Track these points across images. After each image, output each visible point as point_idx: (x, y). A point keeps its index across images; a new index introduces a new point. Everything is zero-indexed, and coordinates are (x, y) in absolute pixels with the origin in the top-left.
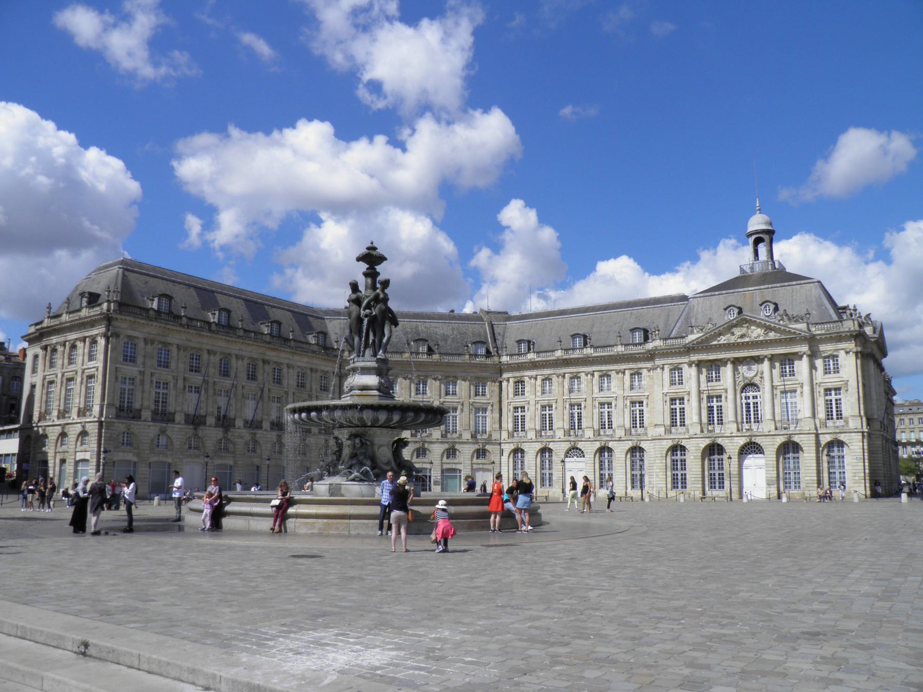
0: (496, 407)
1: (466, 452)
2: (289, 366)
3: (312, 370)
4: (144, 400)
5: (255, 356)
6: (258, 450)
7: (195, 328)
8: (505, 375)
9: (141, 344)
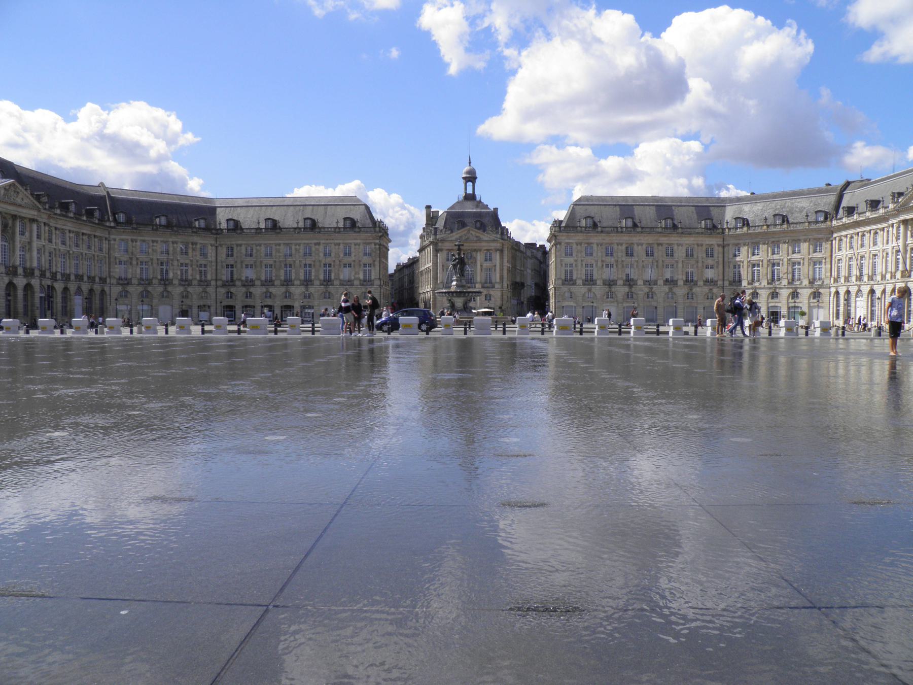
1: (805, 294)
2: (678, 245)
3: (698, 245)
4: (579, 274)
6: (655, 298)
7: (608, 233)
8: (835, 235)
9: (574, 246)
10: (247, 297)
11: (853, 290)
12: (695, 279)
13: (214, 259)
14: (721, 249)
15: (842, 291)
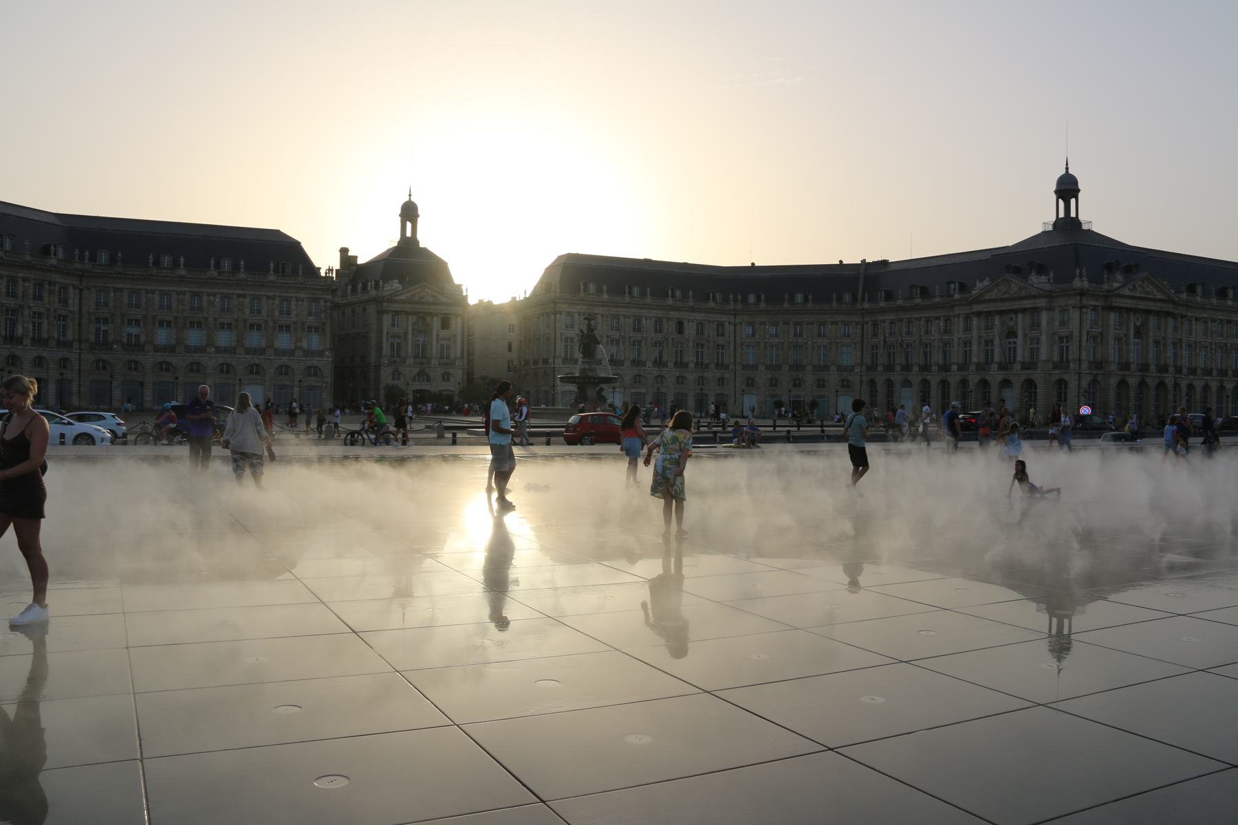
10: (130, 369)
11: (897, 378)
12: (706, 361)
13: (77, 308)
14: (732, 328)
15: (880, 380)
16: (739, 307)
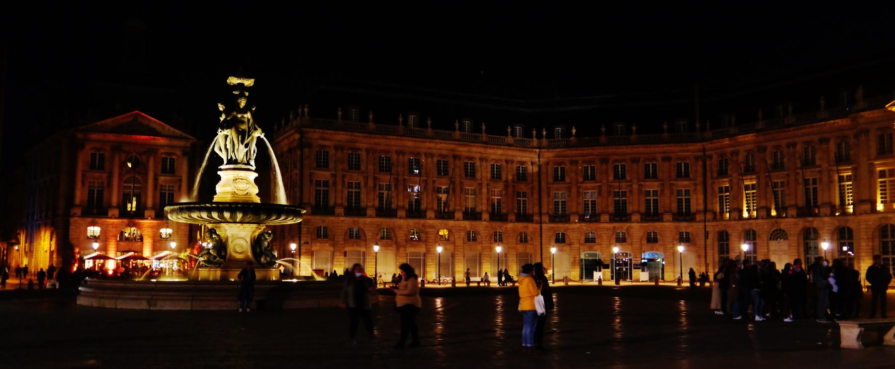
0: (700, 188)
3: (507, 161)
5: (445, 152)
16: (545, 142)
